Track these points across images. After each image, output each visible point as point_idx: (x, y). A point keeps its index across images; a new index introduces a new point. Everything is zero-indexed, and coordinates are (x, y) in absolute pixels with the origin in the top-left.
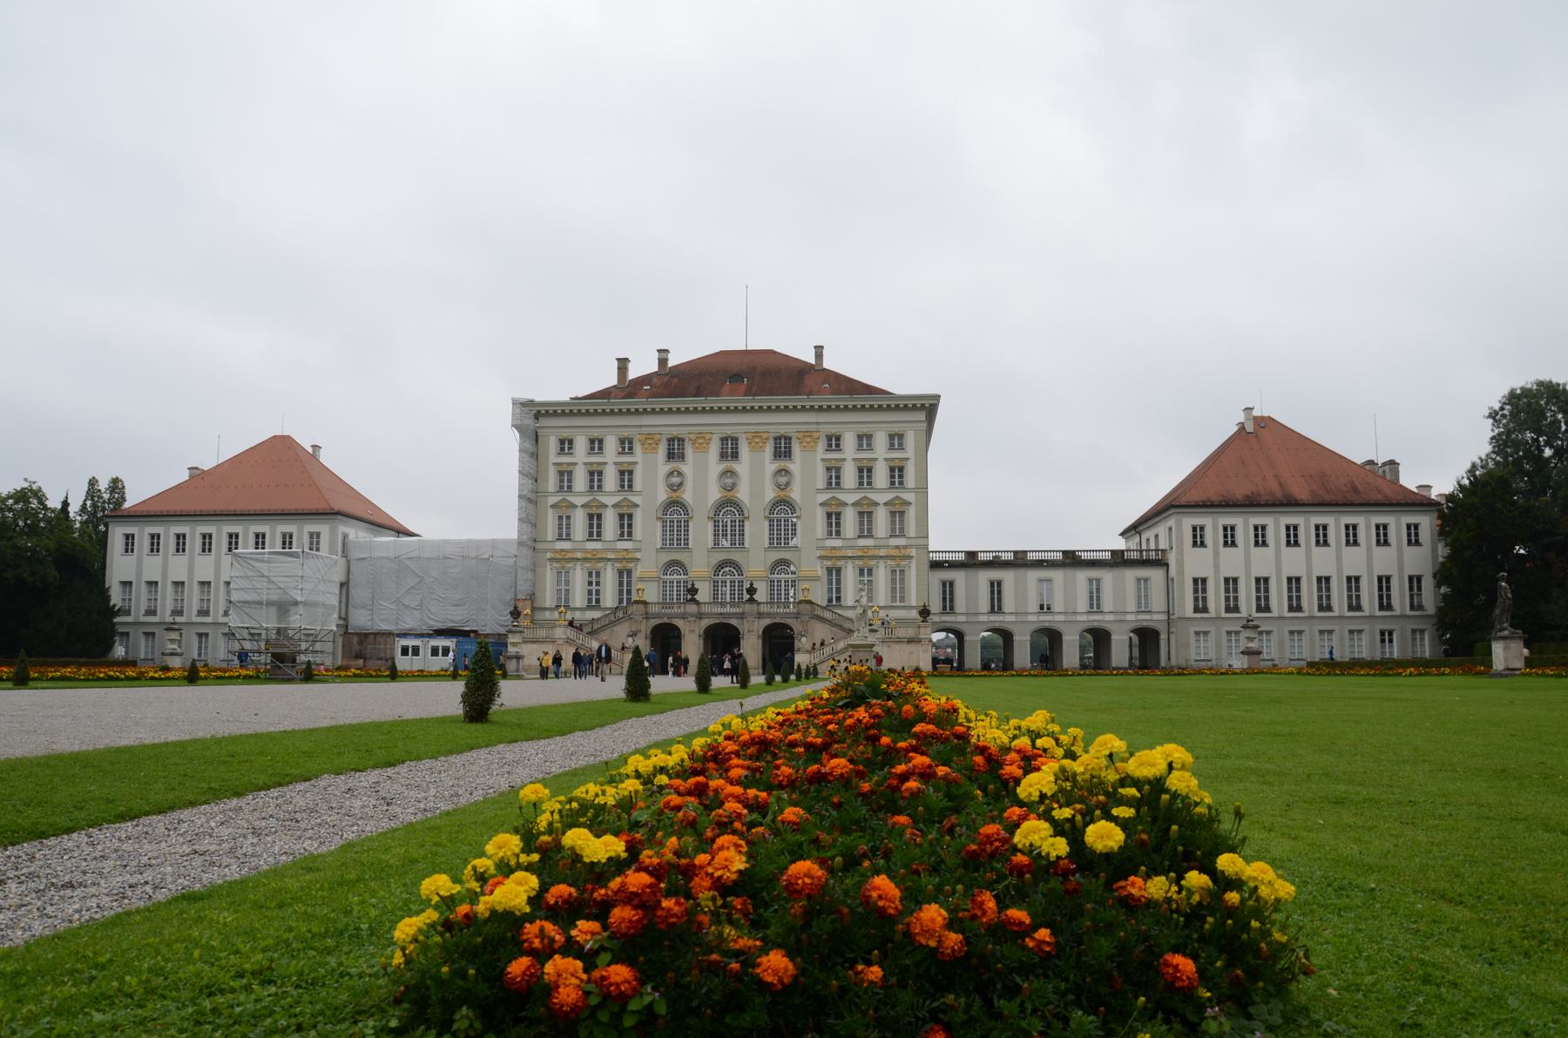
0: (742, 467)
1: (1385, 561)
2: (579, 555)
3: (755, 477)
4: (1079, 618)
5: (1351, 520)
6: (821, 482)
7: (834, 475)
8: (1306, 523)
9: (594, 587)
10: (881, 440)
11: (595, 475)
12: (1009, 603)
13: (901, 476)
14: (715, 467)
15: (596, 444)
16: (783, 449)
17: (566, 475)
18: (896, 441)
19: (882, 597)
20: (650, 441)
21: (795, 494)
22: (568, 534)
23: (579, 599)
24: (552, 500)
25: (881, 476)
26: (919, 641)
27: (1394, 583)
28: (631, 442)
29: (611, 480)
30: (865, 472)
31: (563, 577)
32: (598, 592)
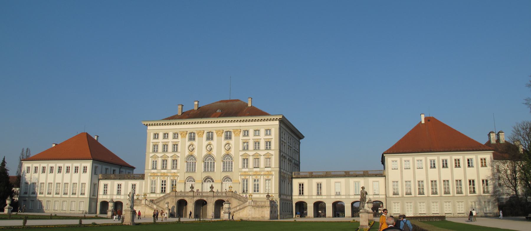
0: (214, 143)
1: (471, 174)
2: (159, 174)
3: (218, 147)
4: (351, 197)
5: (457, 157)
6: (241, 148)
8: (438, 158)
9: (164, 186)
11: (165, 146)
12: (324, 191)
13: (270, 145)
14: (205, 143)
15: (166, 136)
16: (228, 137)
17: (155, 146)
18: (268, 132)
21: (232, 152)
22: (156, 167)
23: (159, 190)
24: (151, 155)
25: (262, 145)
26: (266, 206)
27: (476, 183)
28: (177, 135)
30: (257, 144)
31: (153, 183)
32: (165, 188)
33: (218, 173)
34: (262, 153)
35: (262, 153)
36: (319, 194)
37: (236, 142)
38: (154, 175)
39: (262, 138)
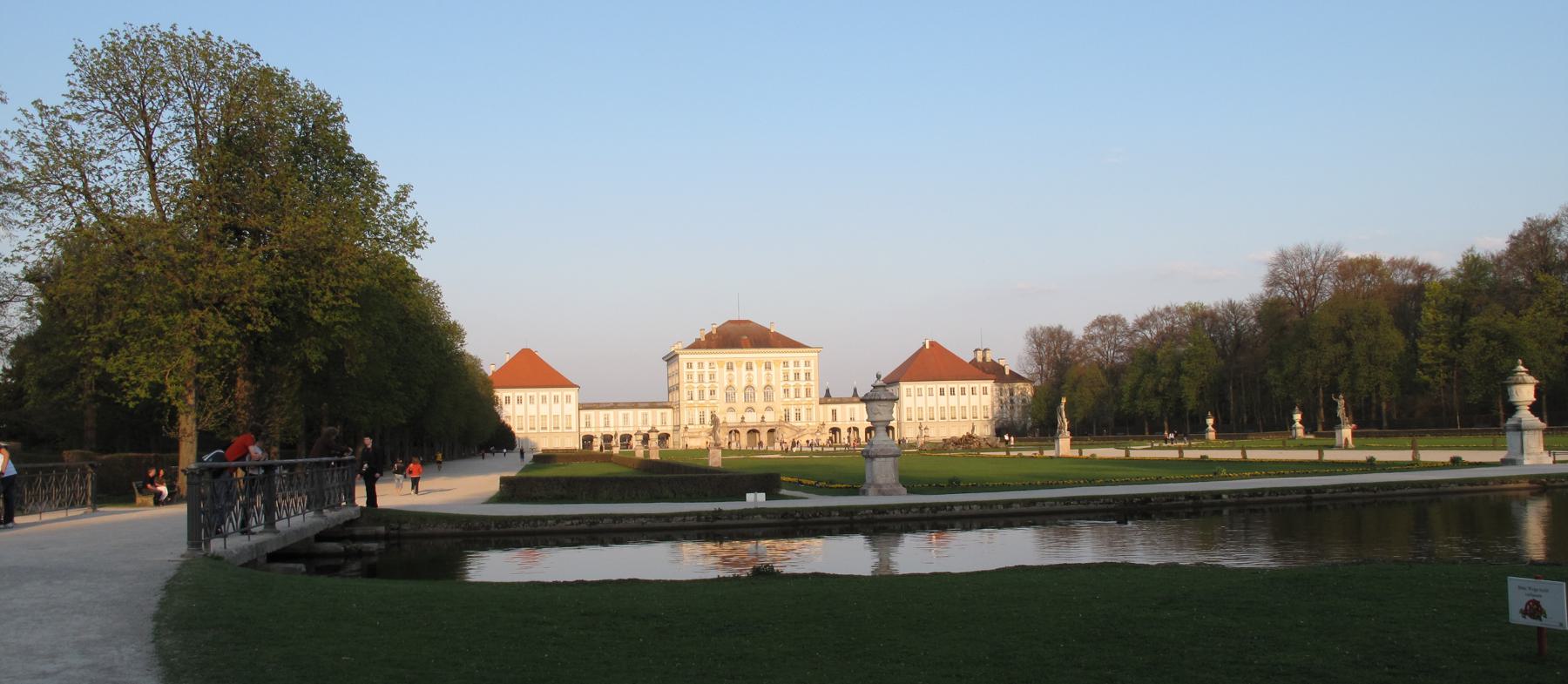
7: (786, 377)
8: (947, 385)
10: (802, 363)
11: (701, 376)
14: (744, 372)
15: (701, 365)
16: (768, 367)
17: (690, 376)
18: (807, 364)
19: (803, 417)
20: (720, 363)
21: (773, 383)
25: (802, 376)
29: (707, 378)
30: (797, 375)
33: (759, 402)
34: (803, 383)
35: (803, 383)
36: (835, 419)
37: (777, 373)
38: (691, 406)
39: (802, 369)
